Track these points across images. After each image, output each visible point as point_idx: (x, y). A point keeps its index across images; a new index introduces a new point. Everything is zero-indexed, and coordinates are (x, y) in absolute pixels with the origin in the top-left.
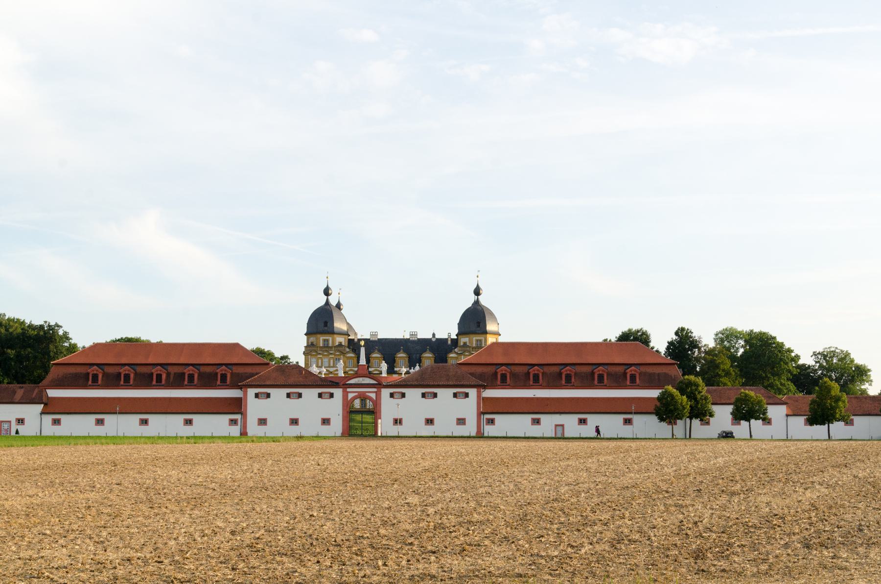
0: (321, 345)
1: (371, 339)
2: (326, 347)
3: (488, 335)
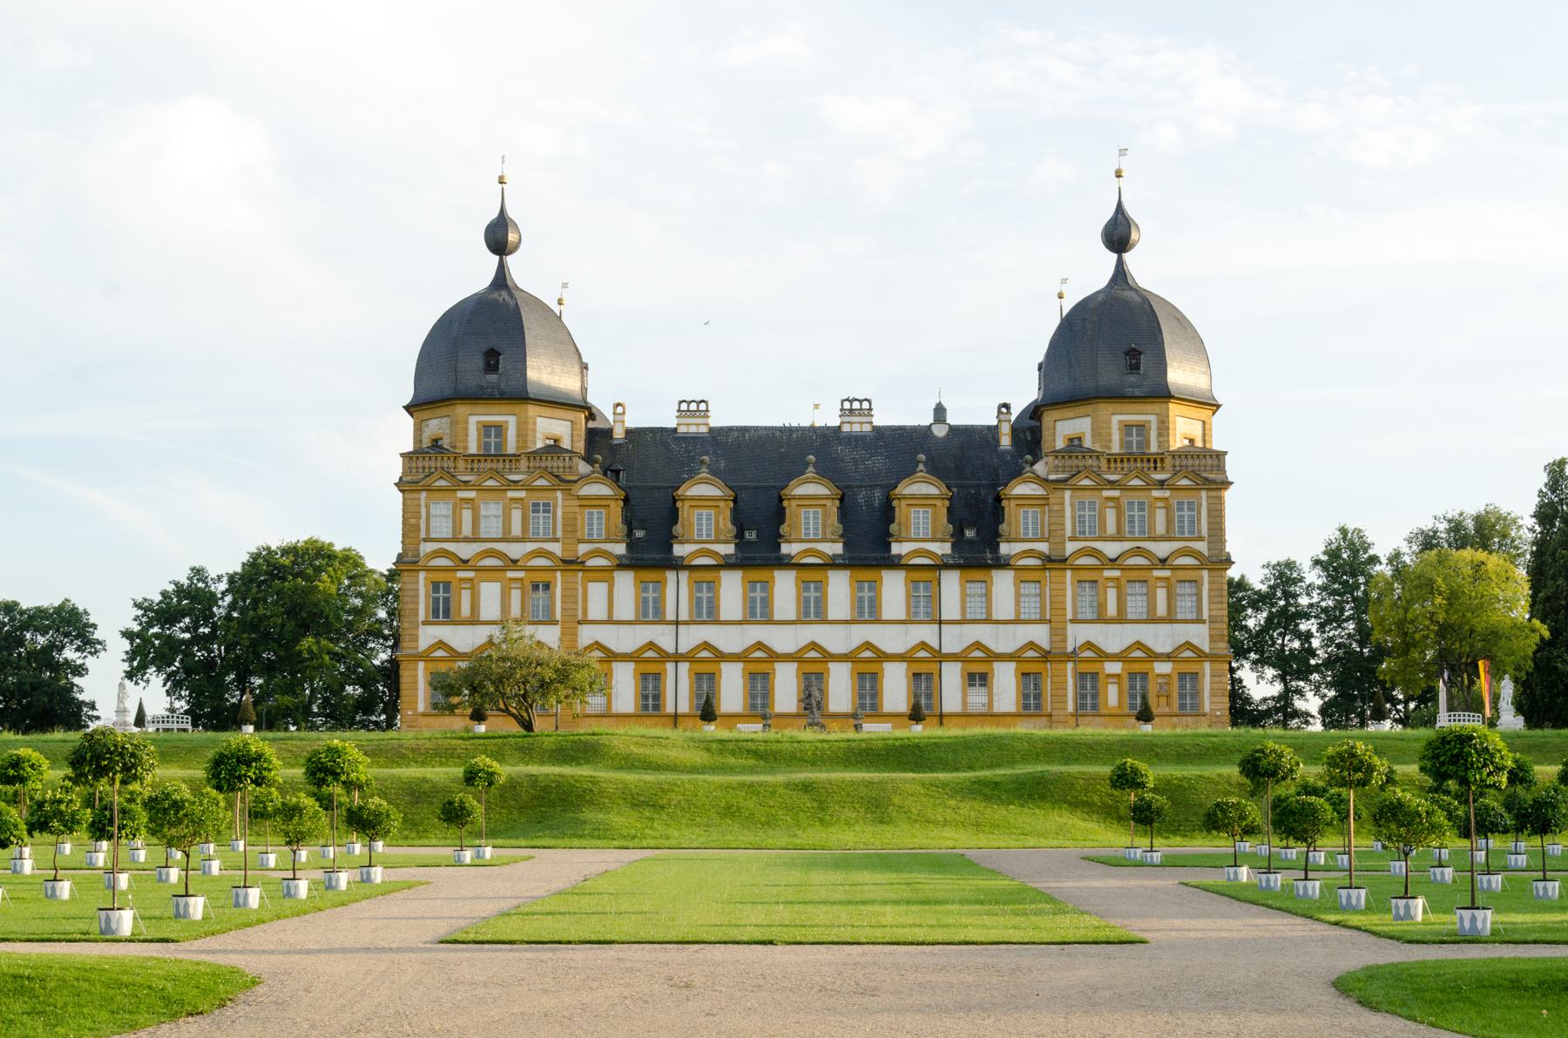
0: (473, 448)
1: (682, 429)
2: (494, 457)
3: (1171, 406)
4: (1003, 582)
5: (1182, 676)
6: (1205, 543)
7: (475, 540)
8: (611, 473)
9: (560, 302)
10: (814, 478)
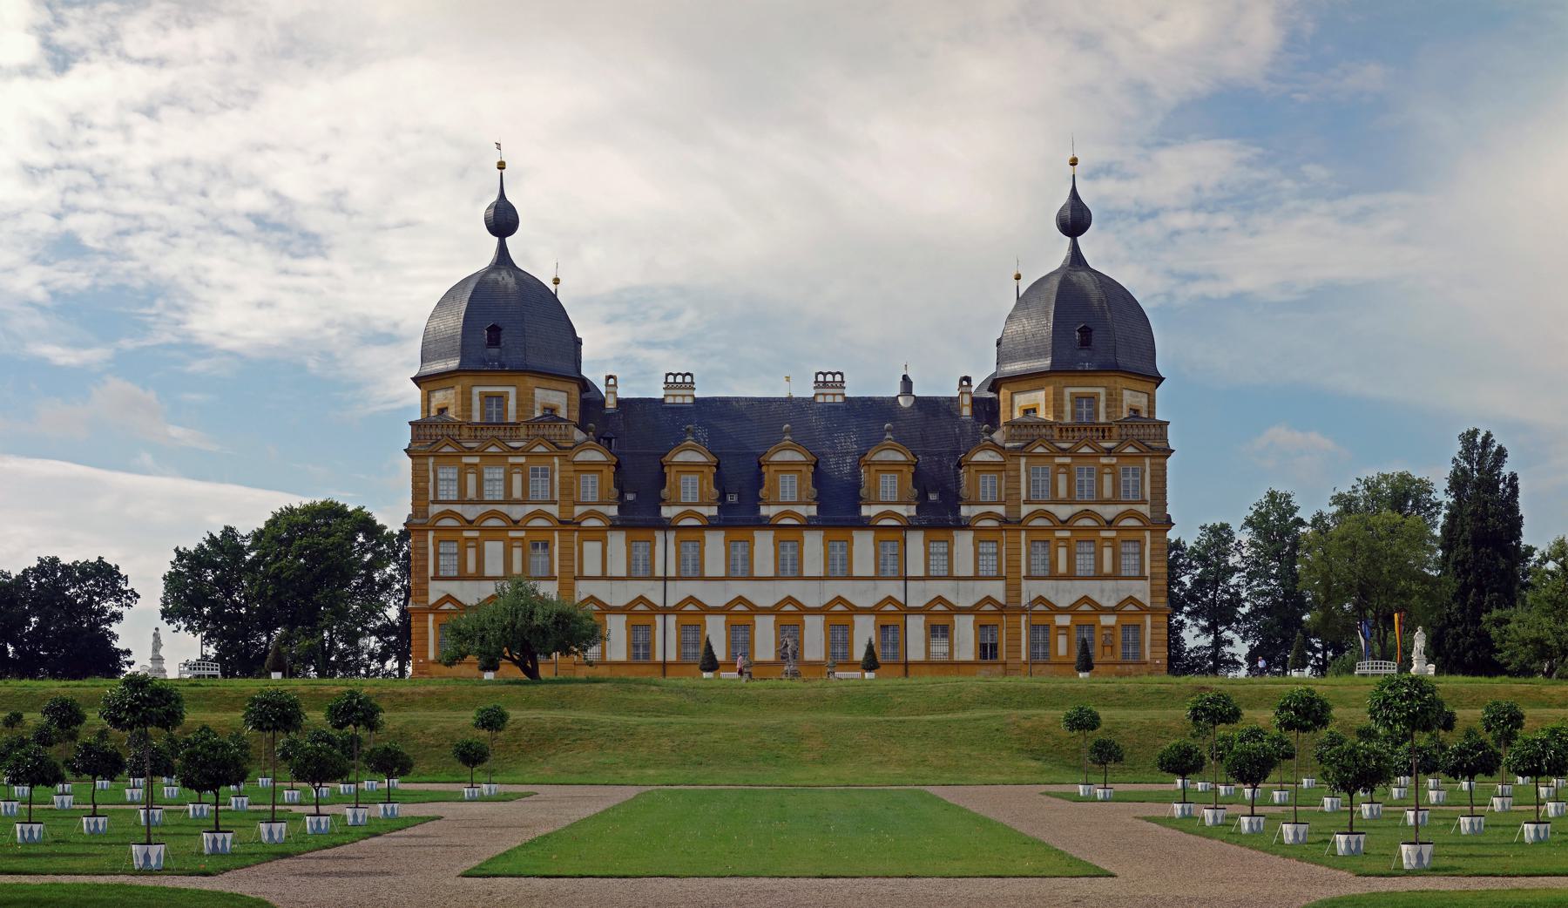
0: (476, 418)
1: (669, 400)
4: (964, 542)
5: (1125, 627)
6: (1148, 506)
7: (481, 502)
8: (603, 440)
9: (556, 281)
10: (791, 445)
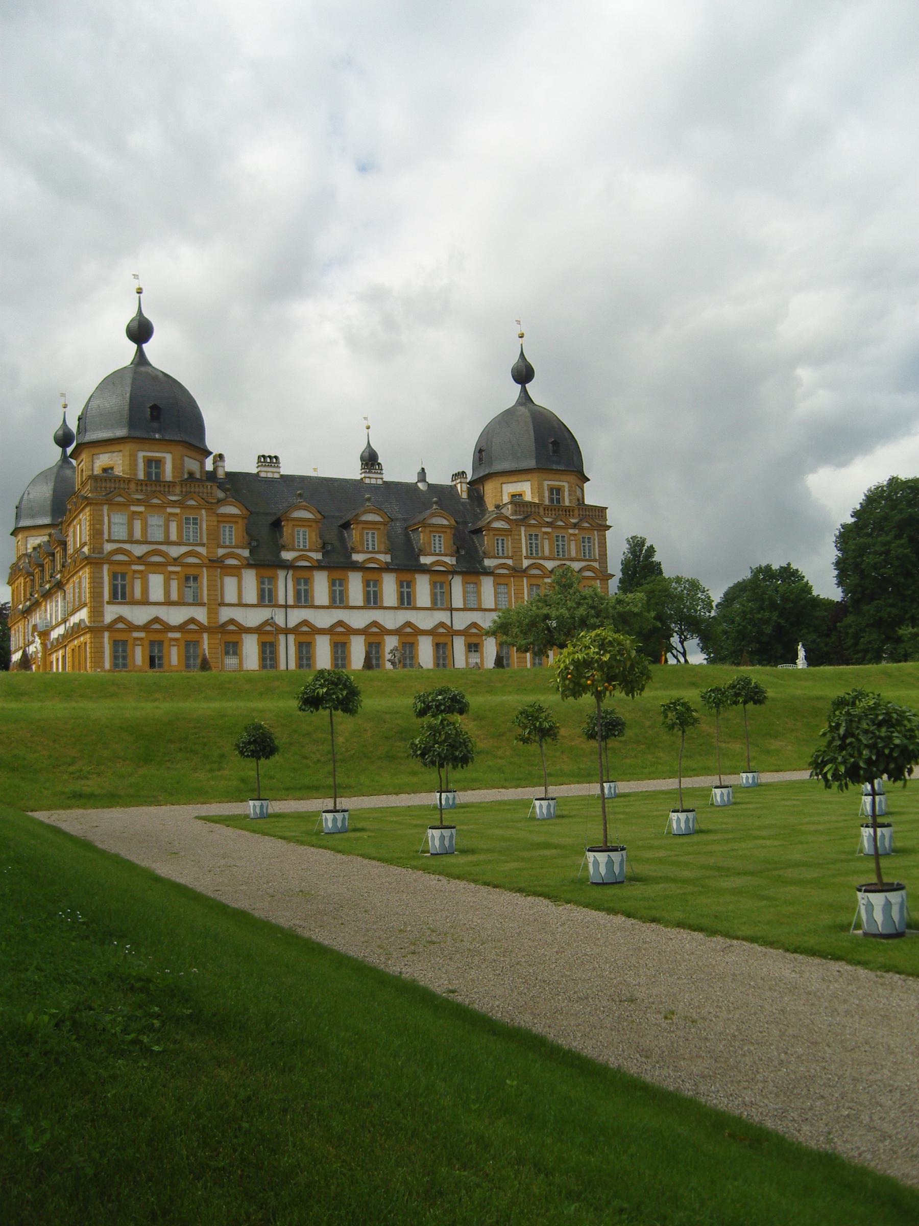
4: (487, 585)
6: (598, 563)
